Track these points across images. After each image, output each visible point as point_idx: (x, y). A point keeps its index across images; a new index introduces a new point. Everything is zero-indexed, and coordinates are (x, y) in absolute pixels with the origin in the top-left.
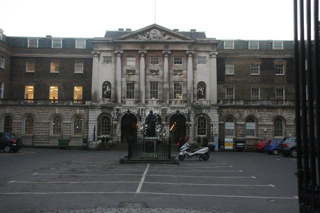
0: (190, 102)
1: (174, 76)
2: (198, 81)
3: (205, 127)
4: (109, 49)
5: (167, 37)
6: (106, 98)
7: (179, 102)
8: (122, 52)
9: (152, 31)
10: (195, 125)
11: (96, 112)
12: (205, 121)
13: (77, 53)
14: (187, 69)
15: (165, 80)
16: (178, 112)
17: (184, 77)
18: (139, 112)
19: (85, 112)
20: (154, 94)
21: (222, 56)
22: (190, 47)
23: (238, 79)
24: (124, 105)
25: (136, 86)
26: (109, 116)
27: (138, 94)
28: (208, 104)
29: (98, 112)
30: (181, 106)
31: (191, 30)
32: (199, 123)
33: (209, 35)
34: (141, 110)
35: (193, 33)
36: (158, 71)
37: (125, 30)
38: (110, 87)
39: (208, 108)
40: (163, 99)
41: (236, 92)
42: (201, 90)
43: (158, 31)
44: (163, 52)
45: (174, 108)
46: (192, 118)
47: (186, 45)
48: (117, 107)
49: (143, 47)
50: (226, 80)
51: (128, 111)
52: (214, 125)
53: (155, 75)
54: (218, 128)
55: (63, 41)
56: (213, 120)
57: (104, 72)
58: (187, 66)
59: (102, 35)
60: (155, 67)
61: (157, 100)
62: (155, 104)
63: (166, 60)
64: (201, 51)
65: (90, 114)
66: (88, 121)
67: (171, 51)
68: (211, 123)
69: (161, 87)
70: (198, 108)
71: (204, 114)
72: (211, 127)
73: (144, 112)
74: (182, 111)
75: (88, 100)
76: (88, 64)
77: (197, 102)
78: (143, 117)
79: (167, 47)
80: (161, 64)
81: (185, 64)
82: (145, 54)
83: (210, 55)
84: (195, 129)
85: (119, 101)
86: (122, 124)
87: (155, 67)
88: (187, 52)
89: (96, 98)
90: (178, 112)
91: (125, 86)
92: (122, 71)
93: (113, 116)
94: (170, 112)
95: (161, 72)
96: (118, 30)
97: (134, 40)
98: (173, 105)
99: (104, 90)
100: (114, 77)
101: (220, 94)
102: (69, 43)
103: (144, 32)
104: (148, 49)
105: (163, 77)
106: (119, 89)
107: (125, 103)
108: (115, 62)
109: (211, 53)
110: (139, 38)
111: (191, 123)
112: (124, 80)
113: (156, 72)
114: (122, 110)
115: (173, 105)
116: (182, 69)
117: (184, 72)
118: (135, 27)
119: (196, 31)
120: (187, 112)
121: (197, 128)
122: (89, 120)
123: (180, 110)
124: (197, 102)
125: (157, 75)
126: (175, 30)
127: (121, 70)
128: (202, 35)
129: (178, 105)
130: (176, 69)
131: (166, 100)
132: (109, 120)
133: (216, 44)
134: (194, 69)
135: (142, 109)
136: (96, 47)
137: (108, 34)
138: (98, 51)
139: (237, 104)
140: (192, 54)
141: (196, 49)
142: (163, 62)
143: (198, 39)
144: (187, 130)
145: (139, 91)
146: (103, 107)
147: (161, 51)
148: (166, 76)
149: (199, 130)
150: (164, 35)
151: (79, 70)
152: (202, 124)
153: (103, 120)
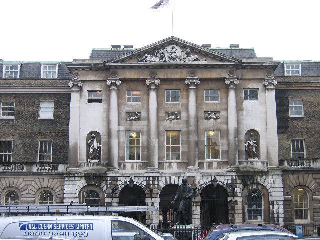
0: (235, 164)
1: (206, 121)
2: (244, 130)
3: (260, 206)
4: (97, 79)
5: (193, 57)
6: (92, 159)
7: (215, 164)
8: (119, 83)
9: (169, 49)
10: (244, 204)
11: (77, 183)
12: (259, 195)
13: (44, 87)
14: (227, 110)
15: (192, 128)
16: (215, 180)
17: (222, 123)
18: (148, 181)
19: (59, 184)
20: (173, 150)
21: (283, 88)
22: (231, 73)
23: (311, 126)
24: (124, 172)
25: (143, 139)
26: (98, 190)
27: (146, 153)
28: (264, 169)
29: (81, 183)
30: (219, 171)
31: (231, 46)
32: (250, 200)
33: (263, 53)
34: (151, 179)
35: (234, 50)
36: (179, 112)
37: (122, 47)
38: (99, 142)
39: (265, 174)
40: (188, 160)
41: (308, 146)
42: (252, 143)
43: (177, 47)
44: (188, 82)
45: (208, 175)
46: (238, 190)
47: (225, 70)
48: (111, 175)
49: (153, 74)
50: (291, 126)
51: (131, 181)
52: (275, 203)
53: (174, 120)
54: (281, 207)
55: (21, 67)
56: (274, 194)
57: (86, 118)
58: (227, 104)
59: (84, 55)
60: (171, 106)
61: (220, 160)
62: (175, 170)
63: (192, 95)
64: (250, 80)
65: (66, 187)
66: (64, 197)
67: (201, 80)
68: (271, 199)
69: (186, 140)
70: (247, 177)
71: (258, 184)
72: (271, 206)
73: (156, 182)
74: (222, 180)
75: (63, 163)
76: (63, 104)
77: (245, 164)
78: (154, 191)
79: (193, 74)
80: (183, 101)
81: (224, 101)
82: (156, 86)
83: (265, 86)
84: (243, 210)
85: (116, 165)
86: (161, 203)
87: (171, 106)
88: (227, 82)
89: (76, 160)
90: (215, 180)
91: (124, 138)
92: (119, 114)
93: (105, 189)
94: (202, 181)
95: (184, 115)
96: (110, 48)
97: (140, 63)
98: (205, 170)
99: (89, 145)
100: (105, 124)
101: (281, 149)
102: (30, 71)
103: (153, 50)
105: (188, 123)
106: (115, 143)
107: (125, 168)
108: (108, 100)
109: (266, 83)
110: (147, 59)
111: (237, 199)
112: (122, 128)
113: (176, 115)
114: (119, 179)
115: (205, 170)
116: (218, 108)
117: (223, 114)
118: (139, 44)
119: (240, 47)
120: (230, 182)
121: (247, 207)
122: (66, 196)
123: (218, 178)
124: (245, 164)
125: (178, 119)
126: (204, 46)
127: (117, 114)
128: (251, 53)
129: (214, 171)
130: (210, 109)
131: (195, 162)
132: (98, 196)
133: (273, 68)
134: (239, 109)
135: (154, 178)
136: (76, 75)
137: (96, 54)
138: (80, 82)
139: (312, 166)
140: (235, 85)
141: (242, 75)
142: (188, 98)
143: (245, 61)
144: (230, 212)
145: (149, 147)
146: (87, 176)
147: (185, 80)
148: (192, 121)
149: (250, 211)
150: (188, 55)
151: (47, 112)
152: (255, 200)
153: (88, 196)
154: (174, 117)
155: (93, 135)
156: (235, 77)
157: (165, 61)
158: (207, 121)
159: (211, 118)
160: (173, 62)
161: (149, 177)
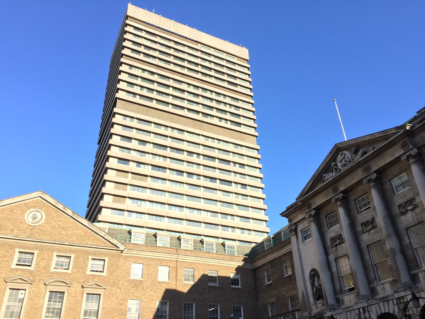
1: (403, 218)
9: (339, 158)
36: (373, 219)
67: (375, 172)
79: (367, 170)
99: (313, 284)
104: (342, 188)
135: (364, 308)
150: (356, 152)
154: (370, 227)
155: (313, 273)
156: (411, 147)
157: (340, 171)
158: (404, 216)
159: (407, 211)
160: (345, 168)
161: (359, 309)
